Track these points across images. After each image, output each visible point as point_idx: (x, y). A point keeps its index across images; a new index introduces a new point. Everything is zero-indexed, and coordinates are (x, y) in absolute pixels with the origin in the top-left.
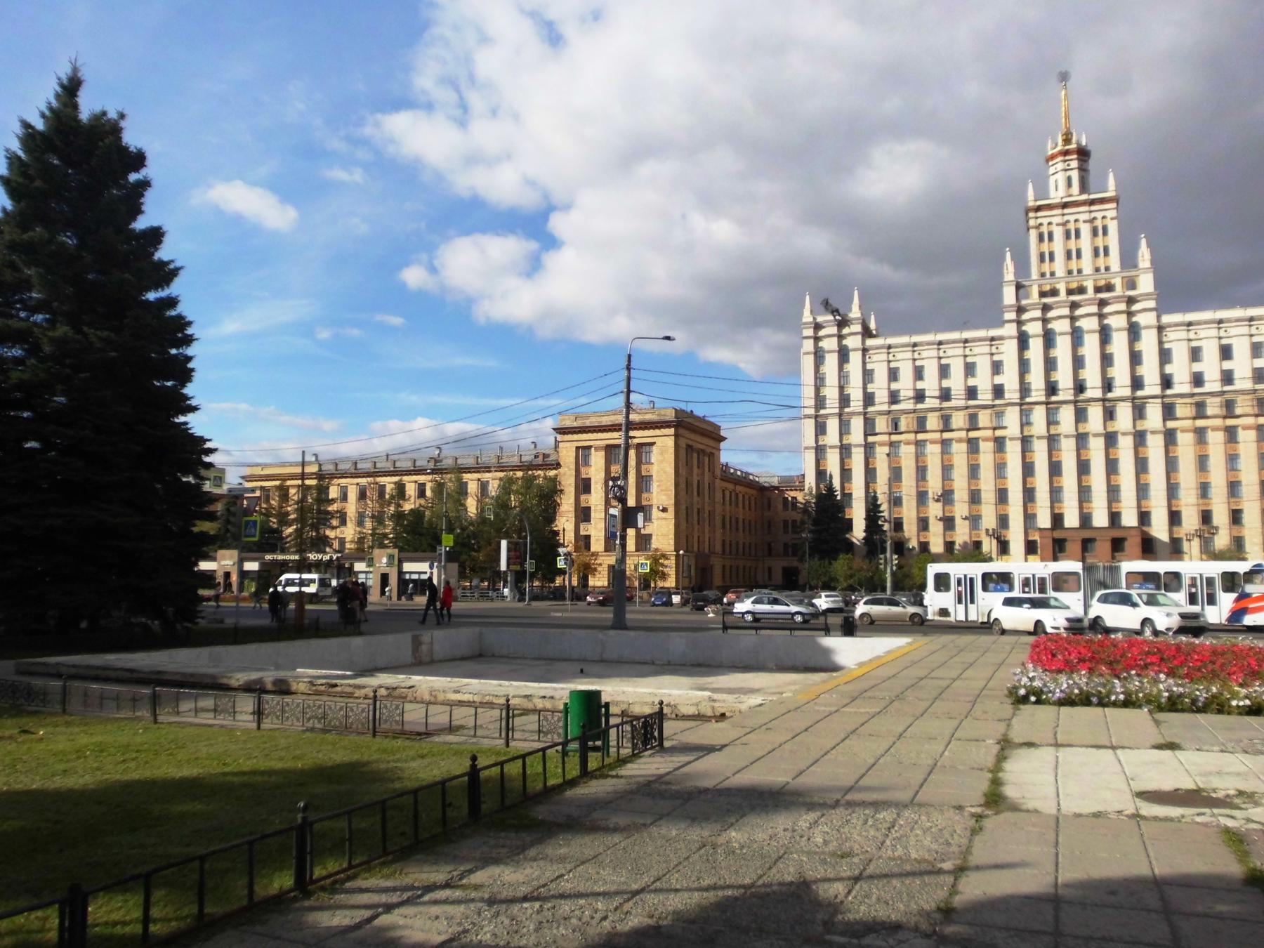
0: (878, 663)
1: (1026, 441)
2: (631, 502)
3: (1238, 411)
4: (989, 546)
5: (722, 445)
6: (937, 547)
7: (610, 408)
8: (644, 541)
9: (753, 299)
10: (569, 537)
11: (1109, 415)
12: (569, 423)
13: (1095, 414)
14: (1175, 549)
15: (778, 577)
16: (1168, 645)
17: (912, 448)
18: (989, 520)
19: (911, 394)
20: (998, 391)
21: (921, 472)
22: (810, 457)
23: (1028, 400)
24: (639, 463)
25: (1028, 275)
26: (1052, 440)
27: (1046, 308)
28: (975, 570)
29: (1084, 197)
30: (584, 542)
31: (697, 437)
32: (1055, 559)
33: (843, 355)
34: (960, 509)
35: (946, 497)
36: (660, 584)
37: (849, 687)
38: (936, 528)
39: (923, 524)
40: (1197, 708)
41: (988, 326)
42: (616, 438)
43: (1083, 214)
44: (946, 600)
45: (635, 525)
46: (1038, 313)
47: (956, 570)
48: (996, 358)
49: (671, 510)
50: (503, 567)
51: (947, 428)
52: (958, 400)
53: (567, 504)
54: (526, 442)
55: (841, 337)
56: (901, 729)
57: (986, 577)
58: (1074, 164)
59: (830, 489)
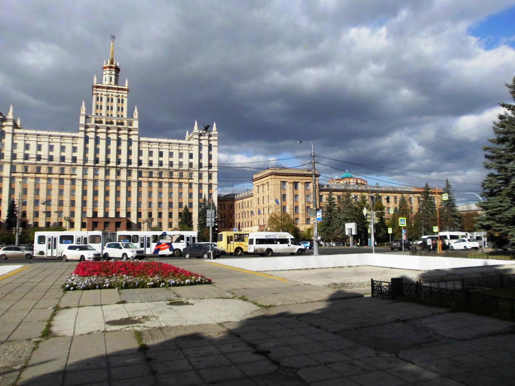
1: (84, 181)
3: (163, 176)
6: (42, 224)
11: (118, 173)
14: (139, 227)
18: (66, 213)
19: (35, 156)
20: (74, 159)
21: (37, 191)
23: (86, 164)
25: (91, 113)
26: (95, 182)
28: (57, 234)
29: (116, 86)
32: (93, 230)
34: (54, 208)
35: (48, 202)
43: (115, 93)
46: (93, 129)
48: (74, 145)
56: (8, 307)
58: (113, 73)
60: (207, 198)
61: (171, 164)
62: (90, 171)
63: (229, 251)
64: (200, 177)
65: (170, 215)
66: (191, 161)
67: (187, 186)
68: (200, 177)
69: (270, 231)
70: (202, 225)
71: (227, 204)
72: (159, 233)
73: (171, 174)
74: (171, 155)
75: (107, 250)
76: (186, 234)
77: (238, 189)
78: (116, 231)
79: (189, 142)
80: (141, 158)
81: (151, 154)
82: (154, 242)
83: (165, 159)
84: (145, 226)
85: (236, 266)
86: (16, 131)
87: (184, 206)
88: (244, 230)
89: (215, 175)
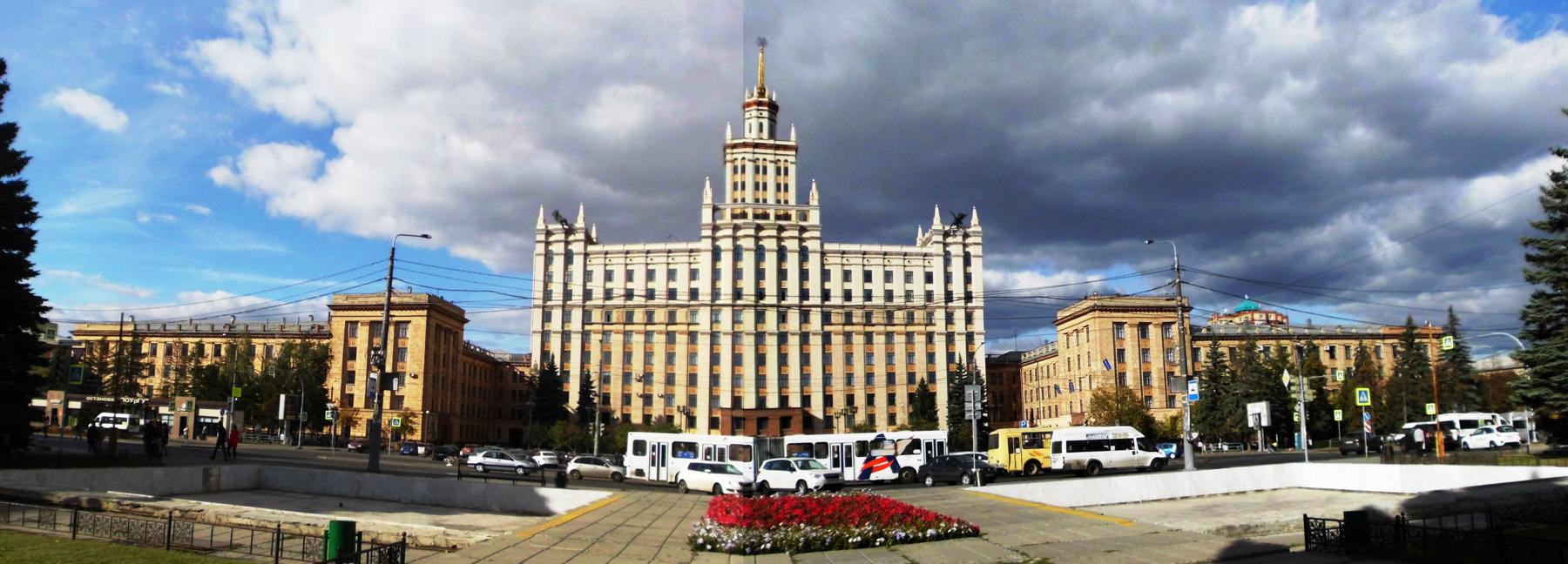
0: (584, 511)
1: (714, 336)
2: (389, 369)
3: (874, 321)
4: (680, 419)
5: (466, 326)
6: (637, 418)
7: (376, 291)
8: (397, 401)
9: (498, 208)
10: (337, 395)
11: (782, 318)
12: (341, 301)
13: (771, 316)
14: (827, 425)
15: (506, 437)
16: (810, 499)
17: (621, 337)
18: (680, 399)
19: (622, 292)
20: (694, 294)
21: (627, 356)
22: (537, 339)
24: (396, 337)
25: (723, 200)
26: (736, 336)
27: (736, 228)
28: (667, 439)
30: (348, 399)
31: (445, 319)
32: (733, 434)
33: (568, 257)
34: (658, 389)
35: (647, 378)
36: (409, 437)
37: (560, 530)
38: (637, 403)
39: (627, 399)
40: (824, 547)
41: (688, 240)
42: (379, 316)
44: (642, 462)
45: (390, 387)
47: (651, 438)
49: (421, 377)
50: (281, 416)
51: (650, 321)
52: (660, 299)
53: (336, 368)
54: (305, 315)
55: (567, 243)
57: (676, 446)
59: (552, 366)
60: (964, 362)
61: (889, 295)
62: (726, 316)
63: (1012, 468)
64: (949, 319)
65: (891, 399)
66: (929, 287)
67: (923, 338)
68: (949, 319)
69: (1096, 424)
70: (956, 417)
71: (1006, 371)
72: (869, 437)
73: (890, 315)
74: (888, 276)
75: (764, 475)
76: (925, 436)
77: (1027, 341)
78: (782, 435)
79: (925, 250)
80: (827, 285)
81: (847, 276)
82: (860, 455)
83: (877, 287)
84: (840, 423)
85: (1028, 498)
86: (591, 248)
87: (918, 379)
88: (1043, 425)
89: (979, 316)
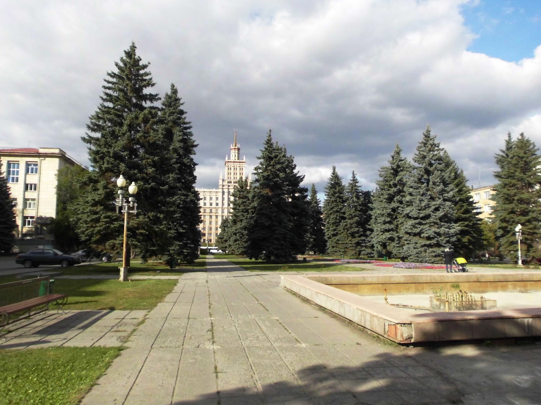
43: (237, 165)
58: (237, 152)
